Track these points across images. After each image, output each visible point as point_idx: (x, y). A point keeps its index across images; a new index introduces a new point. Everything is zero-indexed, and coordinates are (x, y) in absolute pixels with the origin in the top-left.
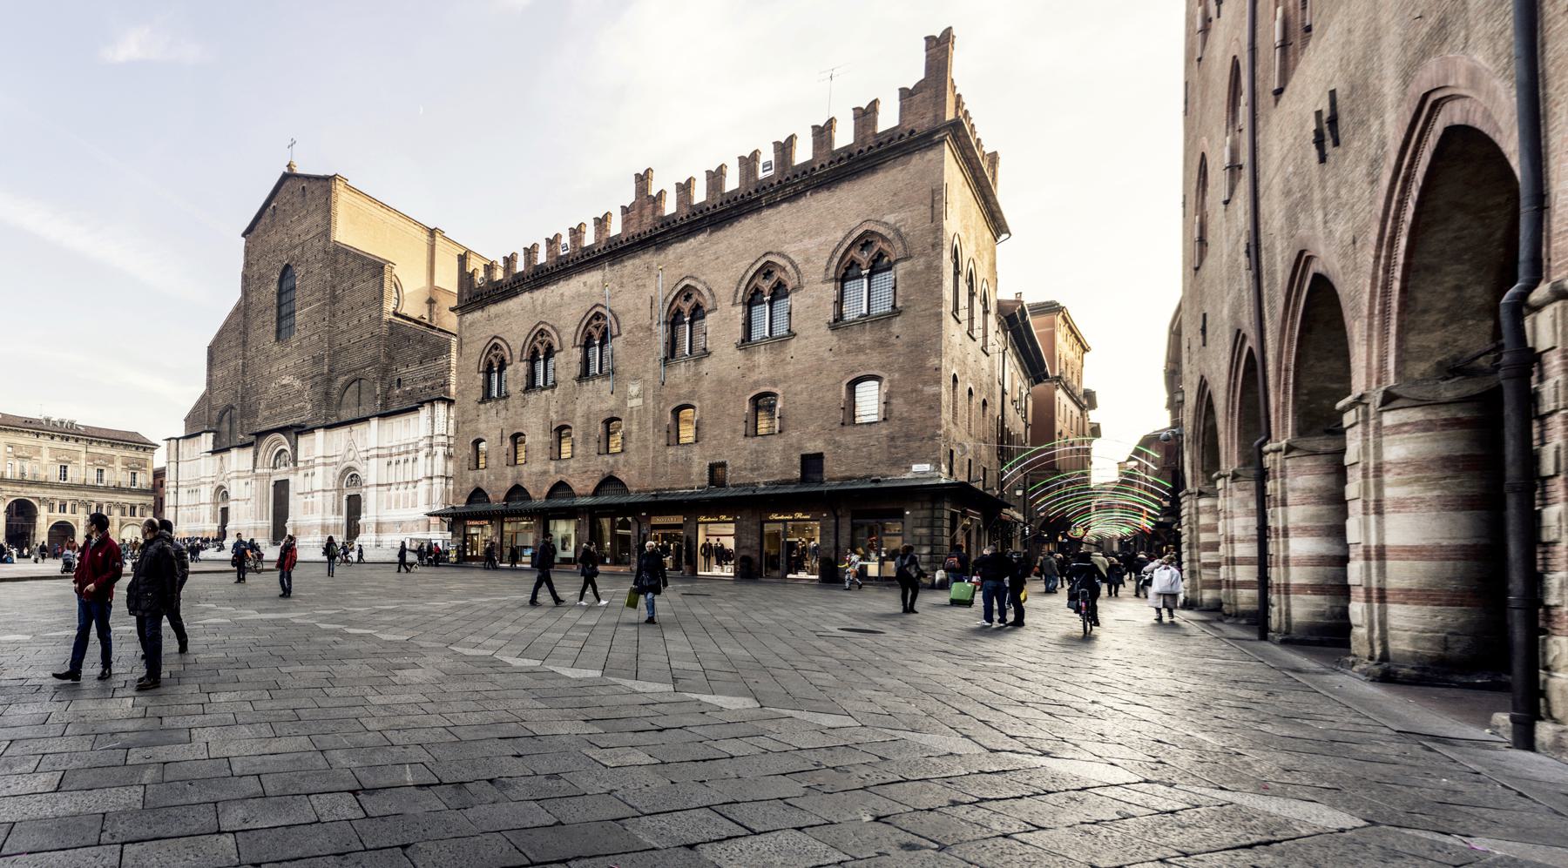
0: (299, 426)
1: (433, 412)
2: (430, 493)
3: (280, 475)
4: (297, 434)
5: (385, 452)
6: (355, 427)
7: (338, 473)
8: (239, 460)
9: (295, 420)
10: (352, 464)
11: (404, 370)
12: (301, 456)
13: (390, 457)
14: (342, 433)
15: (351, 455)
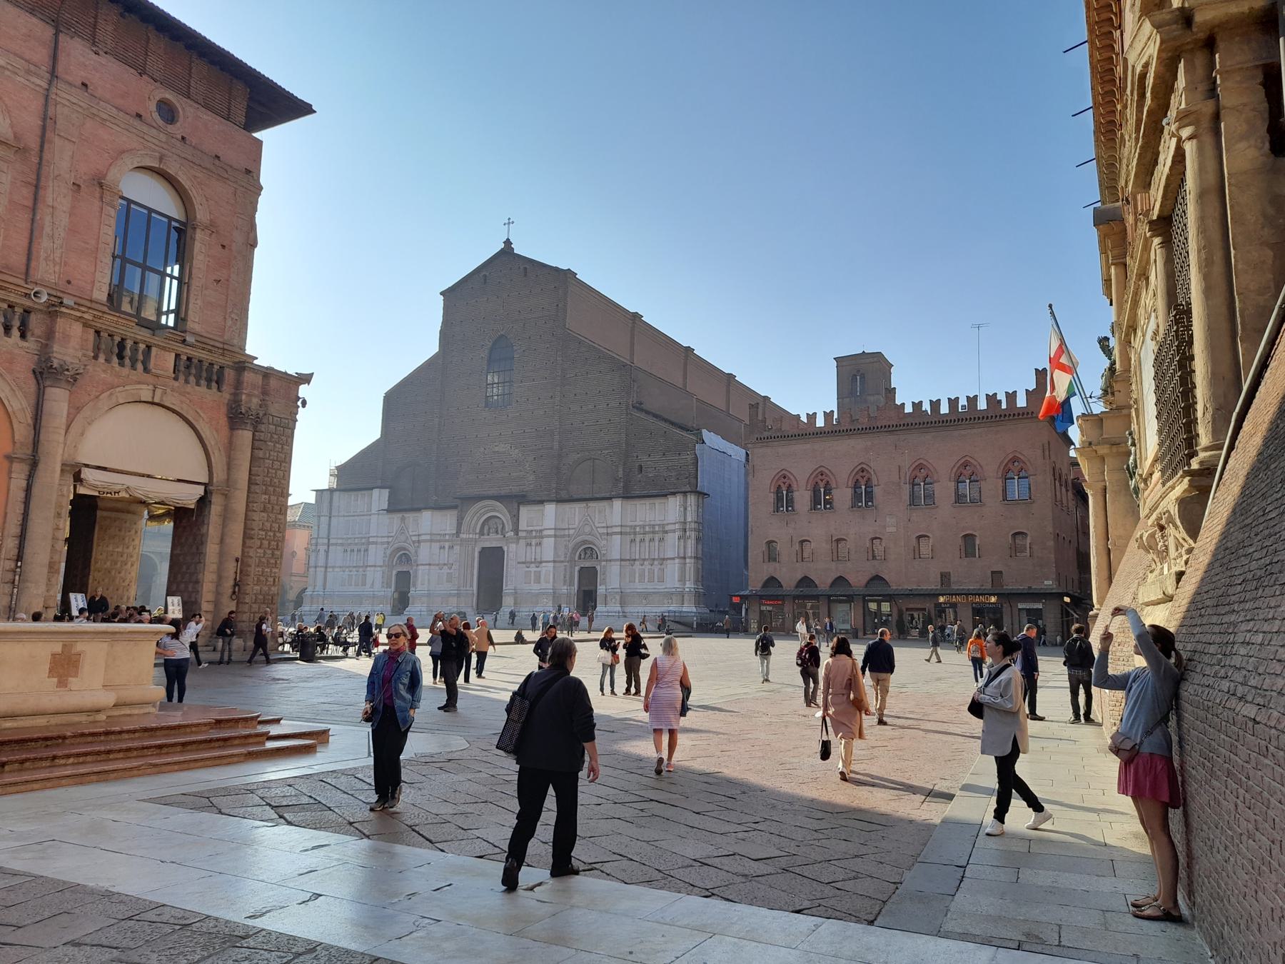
0: (524, 496)
1: (685, 502)
2: (683, 571)
3: (492, 541)
4: (519, 504)
5: (628, 530)
6: (591, 504)
7: (571, 545)
8: (429, 522)
9: (514, 489)
10: (589, 538)
11: (645, 458)
12: (523, 525)
13: (629, 533)
14: (577, 508)
15: (587, 529)
